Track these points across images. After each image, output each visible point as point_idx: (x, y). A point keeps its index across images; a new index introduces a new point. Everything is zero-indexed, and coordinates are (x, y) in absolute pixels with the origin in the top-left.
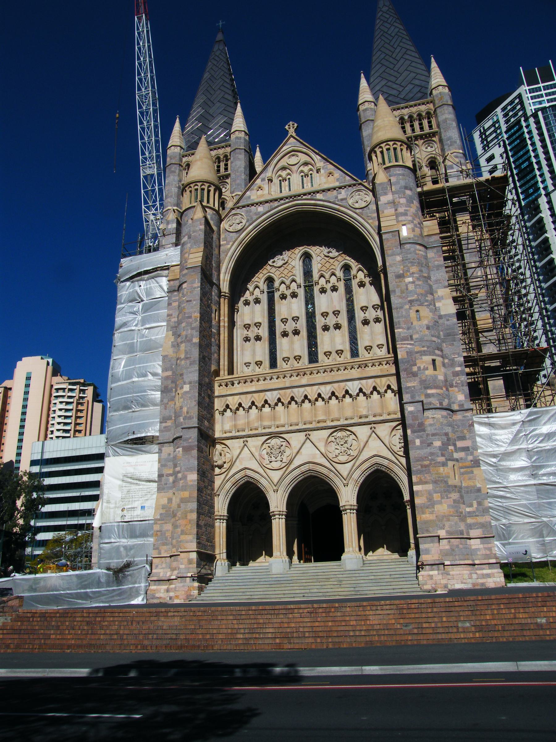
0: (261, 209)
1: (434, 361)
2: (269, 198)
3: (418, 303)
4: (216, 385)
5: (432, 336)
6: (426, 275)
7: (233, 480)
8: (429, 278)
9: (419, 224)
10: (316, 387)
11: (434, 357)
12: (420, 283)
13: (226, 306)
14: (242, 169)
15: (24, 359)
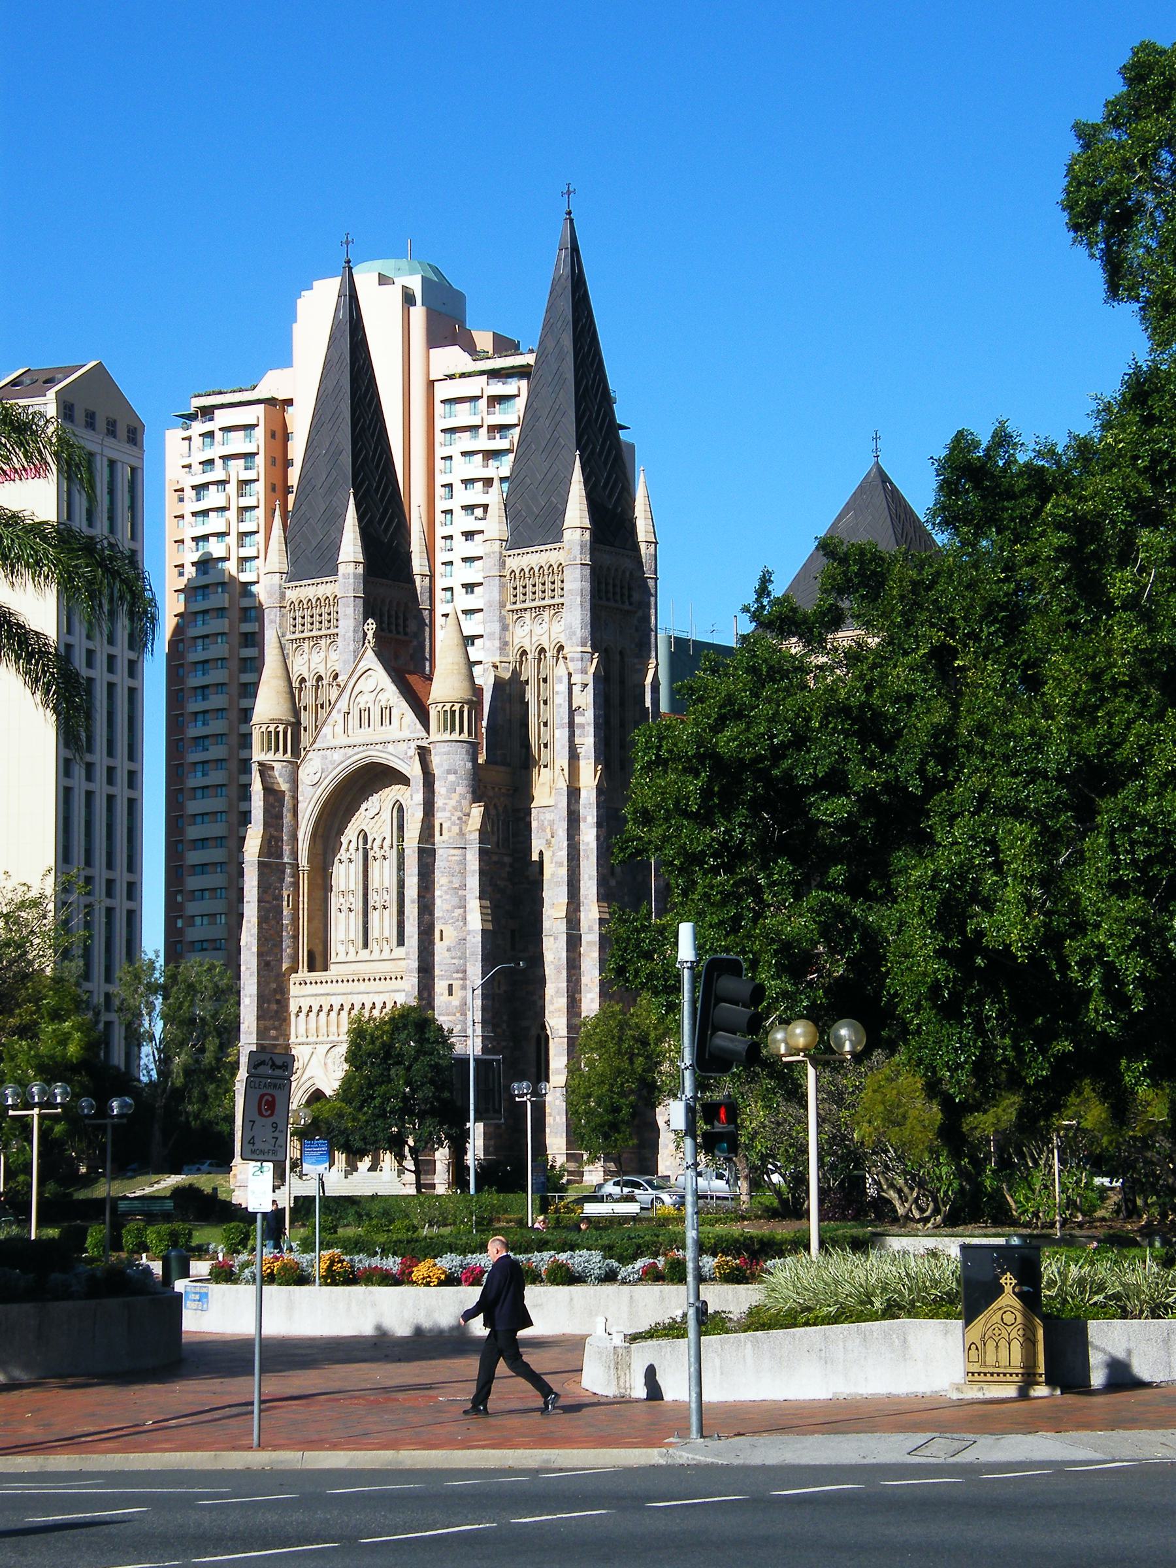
0: (337, 756)
1: (450, 986)
2: (345, 741)
3: (443, 921)
4: (292, 983)
5: (453, 958)
6: (457, 886)
7: (304, 1088)
8: (463, 886)
9: (459, 819)
10: (371, 995)
11: (451, 982)
12: (448, 897)
13: (306, 881)
14: (351, 634)
15: (316, 284)
